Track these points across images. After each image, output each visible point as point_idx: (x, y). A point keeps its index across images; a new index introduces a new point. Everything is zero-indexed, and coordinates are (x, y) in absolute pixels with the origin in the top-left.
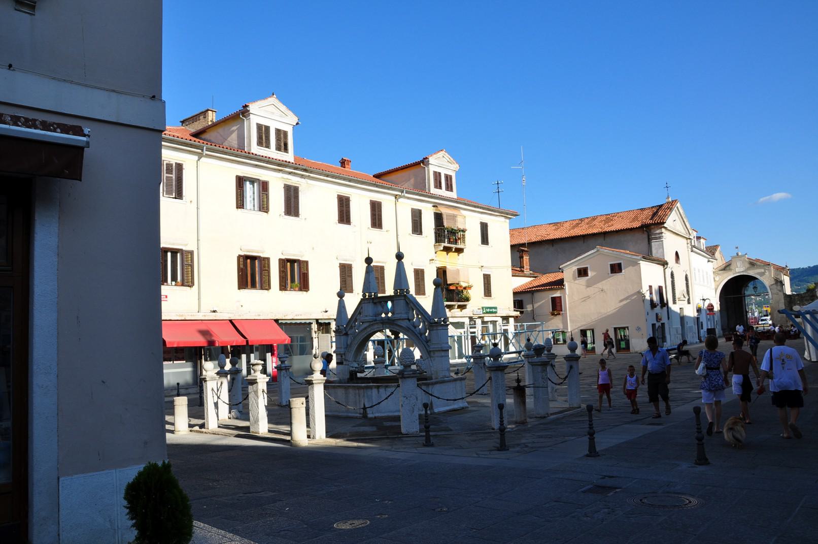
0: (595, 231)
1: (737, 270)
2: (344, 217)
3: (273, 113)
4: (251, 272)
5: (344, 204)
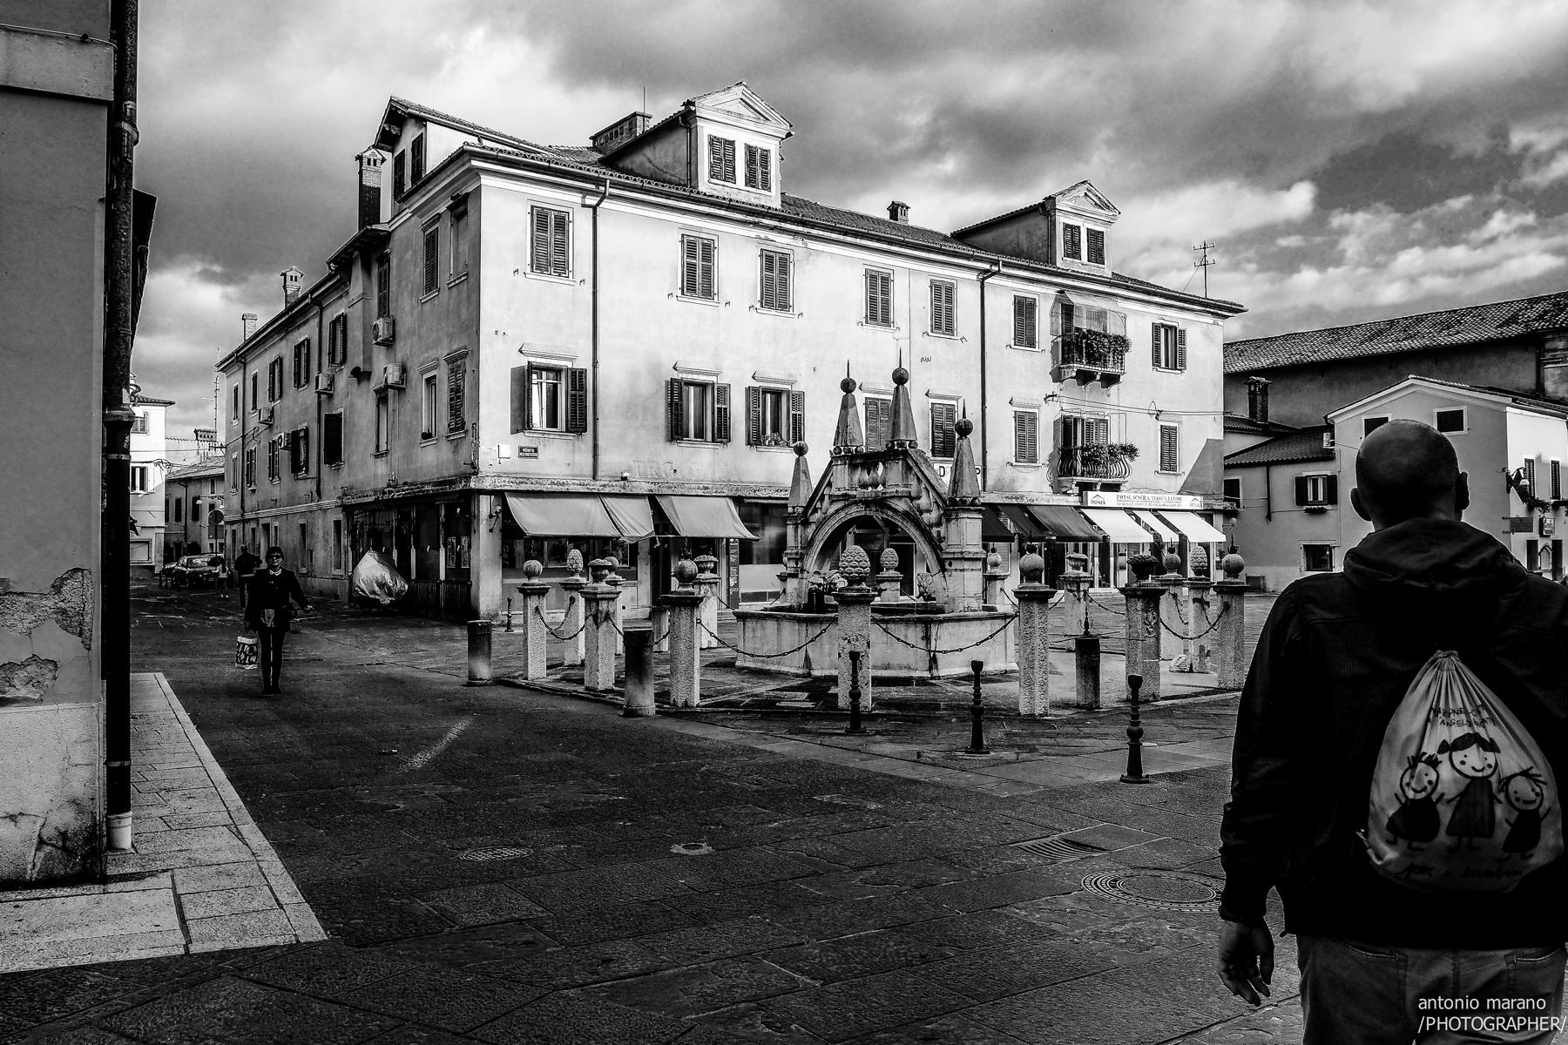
0: (1416, 344)
3: (740, 116)
4: (688, 410)
5: (878, 284)
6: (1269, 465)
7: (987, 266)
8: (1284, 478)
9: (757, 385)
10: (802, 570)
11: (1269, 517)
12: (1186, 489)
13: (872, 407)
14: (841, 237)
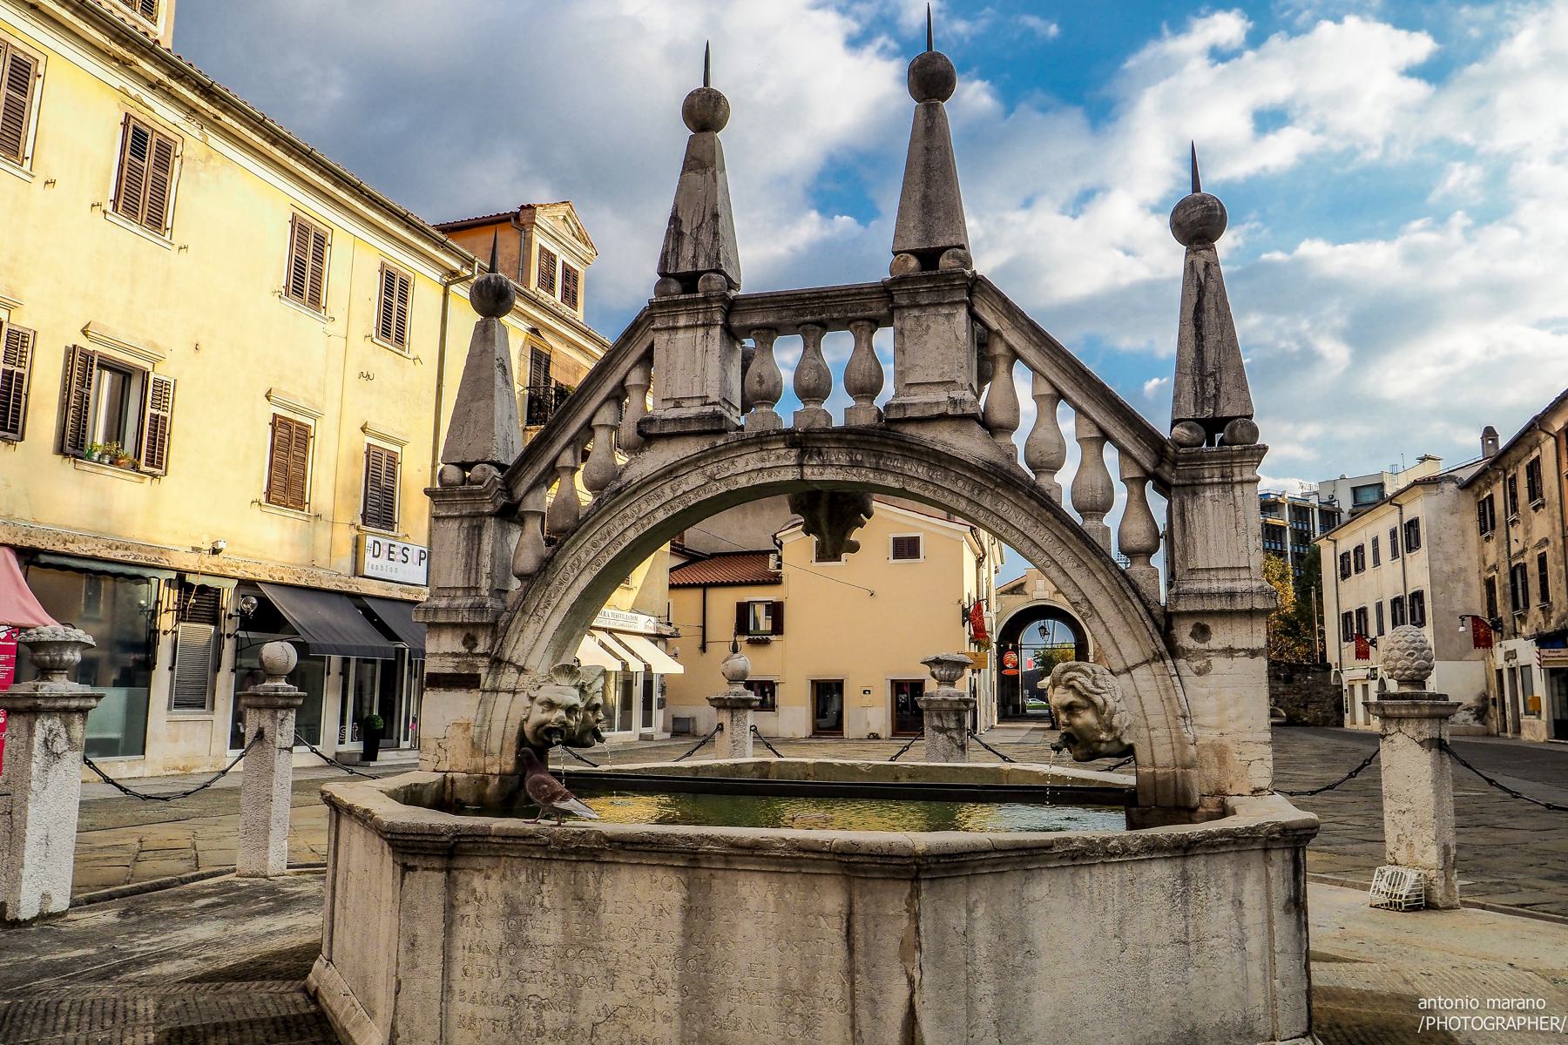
1: (1036, 595)
2: (305, 281)
6: (704, 587)
7: (456, 265)
8: (723, 604)
9: (90, 347)
10: (497, 663)
11: (703, 648)
12: (636, 609)
13: (282, 432)
14: (267, 146)
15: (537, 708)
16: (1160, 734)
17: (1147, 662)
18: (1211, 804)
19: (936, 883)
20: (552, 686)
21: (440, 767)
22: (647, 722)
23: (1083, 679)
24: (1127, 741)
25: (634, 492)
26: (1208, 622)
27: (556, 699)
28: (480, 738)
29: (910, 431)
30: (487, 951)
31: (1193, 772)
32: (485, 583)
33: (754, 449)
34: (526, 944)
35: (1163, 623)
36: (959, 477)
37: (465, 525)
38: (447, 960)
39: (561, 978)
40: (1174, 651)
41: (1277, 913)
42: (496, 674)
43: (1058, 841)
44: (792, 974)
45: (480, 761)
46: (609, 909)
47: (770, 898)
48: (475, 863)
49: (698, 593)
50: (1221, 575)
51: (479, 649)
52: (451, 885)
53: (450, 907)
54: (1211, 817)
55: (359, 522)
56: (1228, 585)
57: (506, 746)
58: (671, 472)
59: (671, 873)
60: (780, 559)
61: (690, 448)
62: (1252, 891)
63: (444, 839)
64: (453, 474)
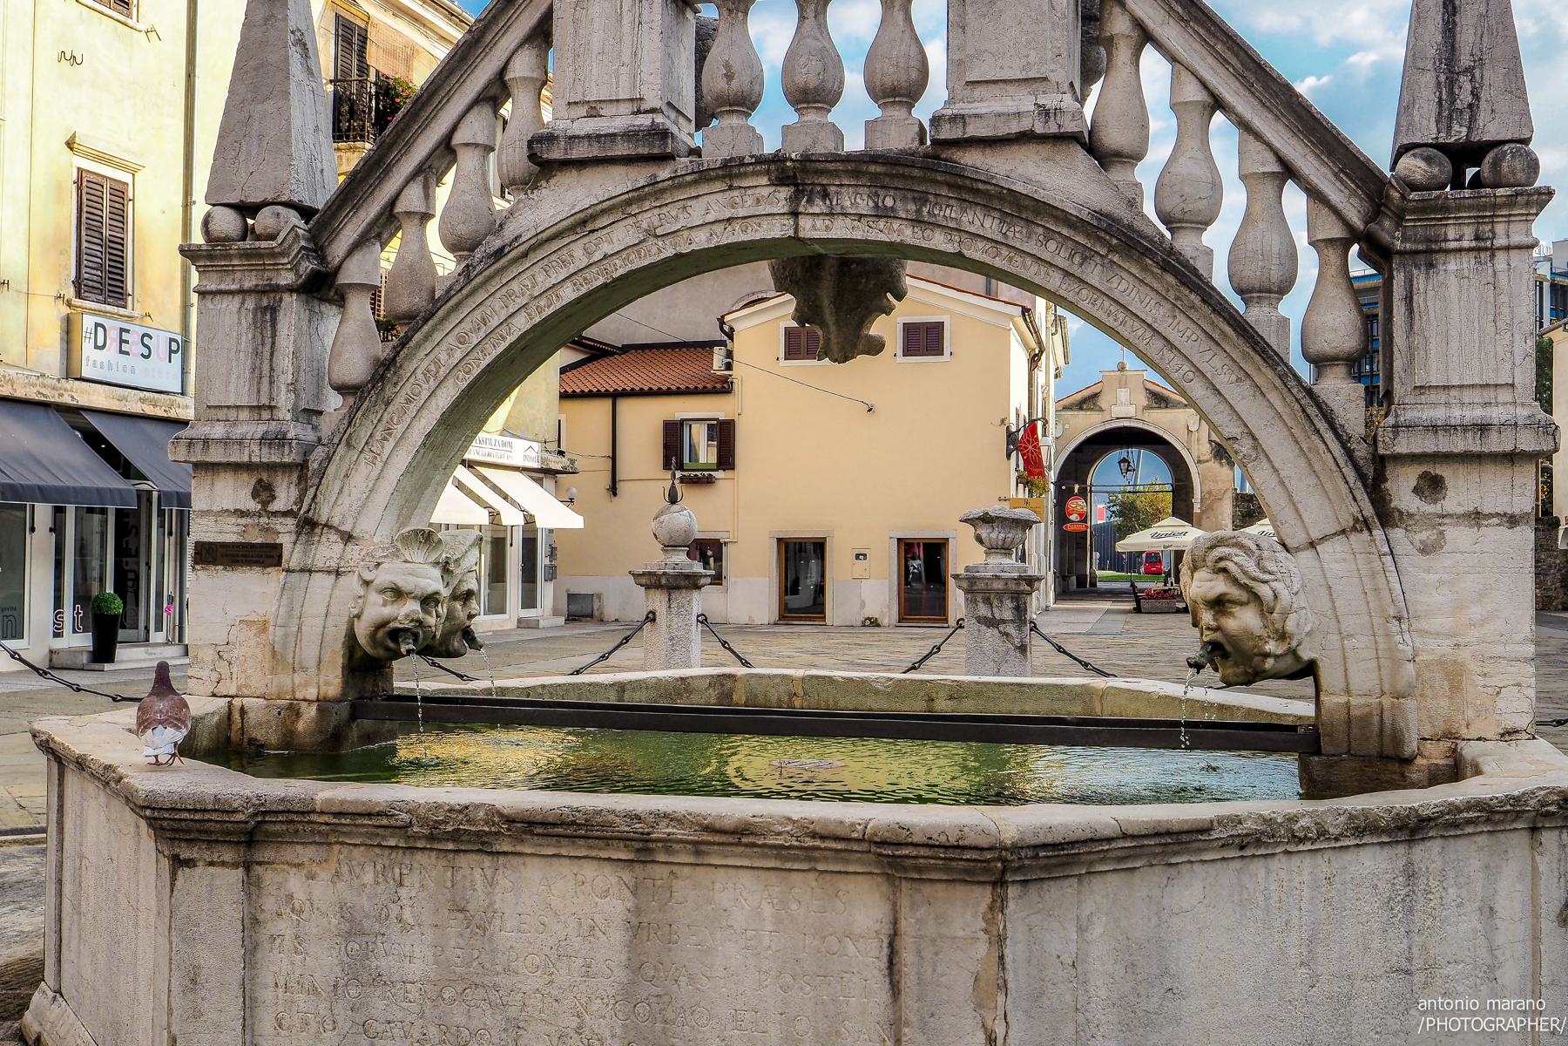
1: (1117, 411)
6: (615, 396)
8: (643, 421)
10: (308, 526)
11: (613, 490)
15: (375, 598)
16: (1360, 645)
17: (1343, 532)
18: (1435, 754)
19: (1033, 888)
20: (398, 564)
21: (222, 690)
22: (529, 601)
23: (1241, 558)
24: (1306, 654)
25: (525, 255)
26: (1440, 470)
27: (406, 583)
28: (285, 645)
29: (971, 159)
30: (314, 991)
31: (1410, 704)
32: (284, 400)
33: (718, 186)
34: (377, 979)
35: (1370, 471)
36: (1049, 234)
37: (250, 303)
38: (249, 1004)
39: (433, 1031)
40: (1386, 516)
41: (1548, 925)
42: (309, 543)
43: (1221, 821)
44: (801, 1027)
45: (285, 680)
46: (508, 925)
47: (767, 910)
48: (289, 853)
49: (602, 408)
50: (1468, 396)
51: (279, 505)
52: (252, 886)
53: (252, 922)
54: (1435, 778)
55: (70, 292)
56: (1475, 414)
57: (326, 658)
58: (584, 222)
59: (608, 869)
60: (729, 354)
61: (616, 182)
62: (1510, 894)
63: (240, 817)
64: (228, 222)
